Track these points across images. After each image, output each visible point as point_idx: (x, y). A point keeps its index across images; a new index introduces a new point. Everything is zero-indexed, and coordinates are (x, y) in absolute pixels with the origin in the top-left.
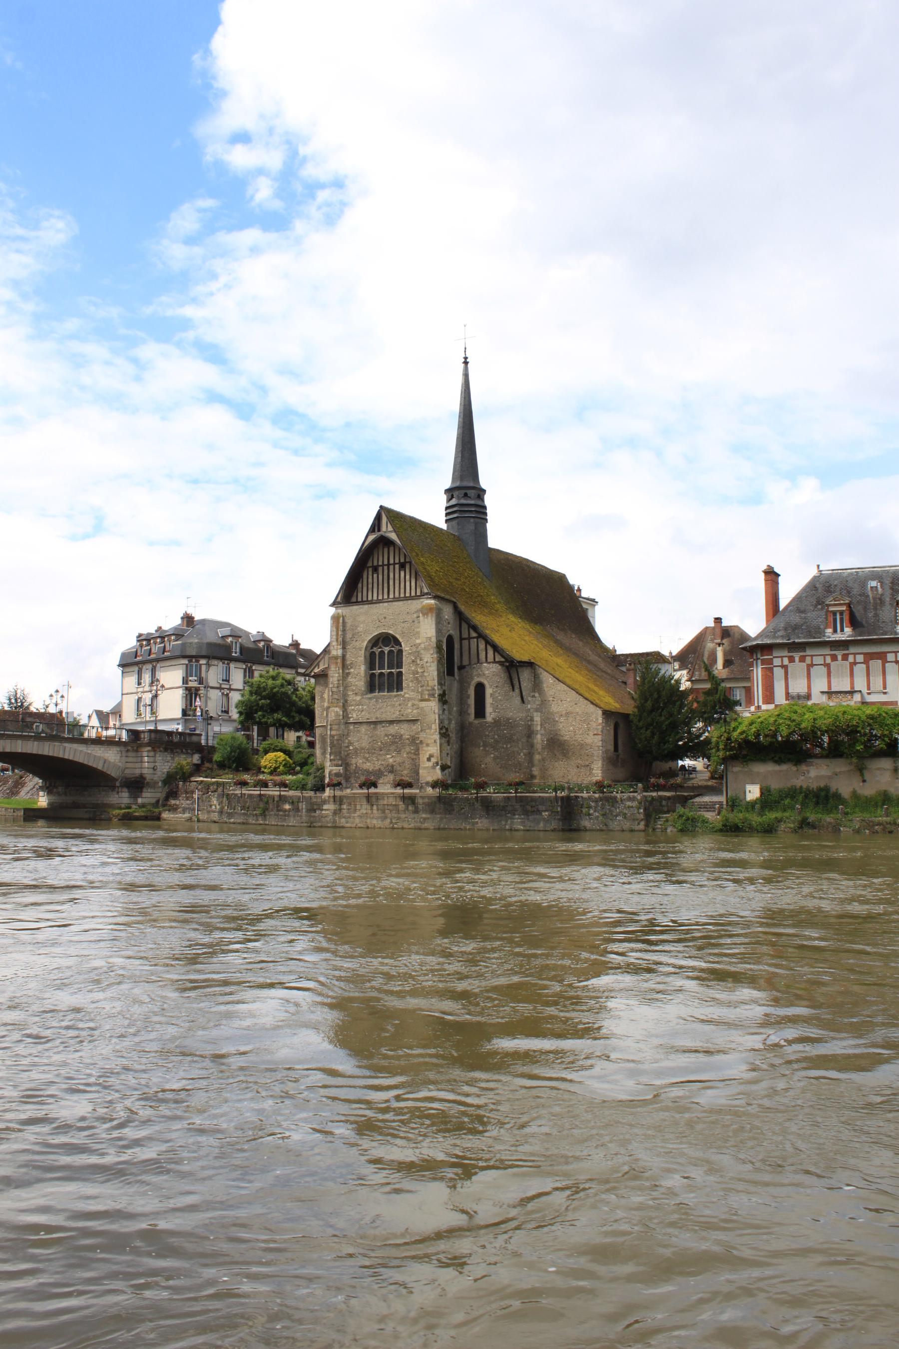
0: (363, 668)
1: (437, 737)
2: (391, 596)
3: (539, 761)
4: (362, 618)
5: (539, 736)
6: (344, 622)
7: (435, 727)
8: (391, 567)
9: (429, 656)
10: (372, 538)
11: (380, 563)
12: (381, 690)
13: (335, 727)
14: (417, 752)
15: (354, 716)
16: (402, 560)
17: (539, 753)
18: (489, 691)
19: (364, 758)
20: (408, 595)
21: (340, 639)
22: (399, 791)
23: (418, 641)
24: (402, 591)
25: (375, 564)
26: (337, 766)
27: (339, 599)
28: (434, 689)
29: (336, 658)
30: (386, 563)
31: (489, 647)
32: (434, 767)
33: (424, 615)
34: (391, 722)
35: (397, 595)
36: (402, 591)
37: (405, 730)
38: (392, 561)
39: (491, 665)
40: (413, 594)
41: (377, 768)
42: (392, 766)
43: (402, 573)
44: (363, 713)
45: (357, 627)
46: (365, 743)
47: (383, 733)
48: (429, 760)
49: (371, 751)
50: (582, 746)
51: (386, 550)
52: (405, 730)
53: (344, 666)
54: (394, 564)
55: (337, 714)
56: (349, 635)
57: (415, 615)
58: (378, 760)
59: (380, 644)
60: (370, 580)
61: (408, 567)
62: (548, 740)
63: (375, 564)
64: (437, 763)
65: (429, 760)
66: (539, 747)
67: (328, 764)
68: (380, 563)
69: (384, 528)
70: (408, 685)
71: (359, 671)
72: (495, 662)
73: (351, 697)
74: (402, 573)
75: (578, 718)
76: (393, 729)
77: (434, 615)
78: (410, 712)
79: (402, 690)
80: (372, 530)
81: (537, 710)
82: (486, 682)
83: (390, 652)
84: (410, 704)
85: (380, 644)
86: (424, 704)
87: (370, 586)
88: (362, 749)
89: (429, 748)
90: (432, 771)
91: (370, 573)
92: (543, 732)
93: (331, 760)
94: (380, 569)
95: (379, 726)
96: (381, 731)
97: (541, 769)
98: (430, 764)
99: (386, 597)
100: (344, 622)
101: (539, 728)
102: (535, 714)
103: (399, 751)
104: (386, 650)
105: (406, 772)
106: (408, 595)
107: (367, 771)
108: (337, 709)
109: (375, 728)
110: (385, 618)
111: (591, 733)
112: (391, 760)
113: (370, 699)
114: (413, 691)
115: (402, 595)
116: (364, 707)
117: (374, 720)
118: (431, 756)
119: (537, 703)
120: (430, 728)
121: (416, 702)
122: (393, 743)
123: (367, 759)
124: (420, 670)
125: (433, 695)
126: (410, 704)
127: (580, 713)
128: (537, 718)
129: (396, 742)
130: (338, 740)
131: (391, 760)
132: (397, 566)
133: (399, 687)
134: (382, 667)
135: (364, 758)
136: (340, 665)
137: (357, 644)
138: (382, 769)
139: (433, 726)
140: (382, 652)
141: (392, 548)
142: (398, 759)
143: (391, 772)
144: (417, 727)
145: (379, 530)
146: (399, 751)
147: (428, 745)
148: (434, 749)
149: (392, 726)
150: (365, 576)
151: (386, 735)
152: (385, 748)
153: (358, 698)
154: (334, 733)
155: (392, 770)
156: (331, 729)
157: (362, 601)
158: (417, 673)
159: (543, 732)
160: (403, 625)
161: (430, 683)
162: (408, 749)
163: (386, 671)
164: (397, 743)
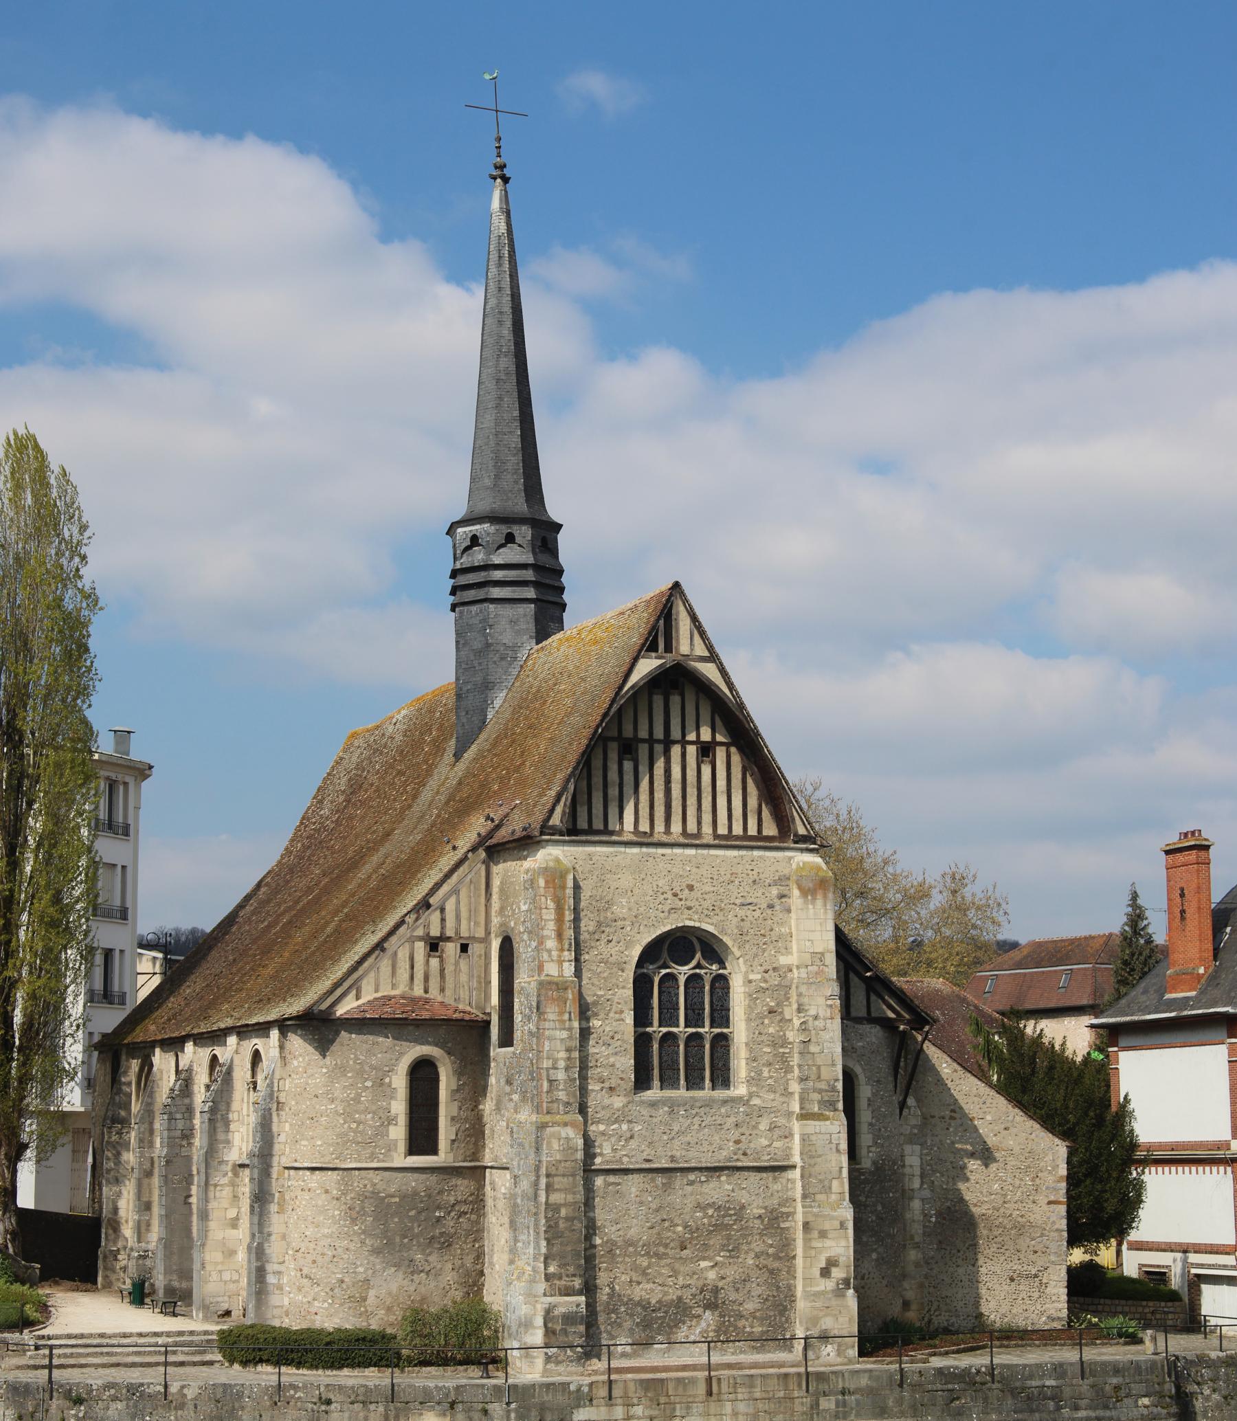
0: (629, 1018)
1: (848, 1213)
2: (676, 827)
3: (917, 1265)
4: (626, 880)
5: (916, 1204)
6: (577, 887)
7: (841, 1186)
8: (676, 751)
9: (821, 1001)
10: (647, 666)
11: (643, 734)
12: (668, 1080)
13: (559, 1182)
14: (785, 1253)
15: (605, 1154)
16: (706, 735)
17: (917, 1246)
18: (865, 1092)
19: (635, 1268)
20: (723, 830)
21: (569, 933)
22: (884, 1366)
23: (784, 960)
24: (707, 817)
25: (628, 732)
26: (568, 1292)
27: (556, 820)
28: (834, 1089)
29: (561, 986)
30: (659, 733)
31: (854, 979)
32: (839, 1293)
33: (804, 892)
34: (715, 1170)
35: (692, 827)
36: (707, 817)
37: (751, 1194)
38: (676, 734)
39: (866, 1028)
40: (738, 830)
41: (673, 1295)
42: (716, 1290)
43: (706, 770)
44: (633, 1144)
45: (609, 903)
46: (637, 1228)
47: (690, 1202)
48: (825, 1272)
49: (655, 1250)
50: (1021, 1229)
51: (658, 701)
52: (751, 1194)
53: (584, 1011)
54: (684, 743)
55: (569, 1148)
56: (587, 925)
57: (775, 891)
58: (675, 1274)
59: (665, 955)
60: (613, 775)
61: (720, 753)
62: (939, 1214)
63: (628, 732)
64: (846, 1282)
65: (825, 1272)
66: (917, 1229)
67: (542, 1286)
68: (643, 734)
69: (684, 648)
70: (760, 1073)
71: (617, 1025)
72: (871, 1020)
73: (597, 1097)
74: (706, 770)
75: (1012, 1162)
76: (718, 1190)
77: (830, 895)
78: (762, 1145)
79: (726, 1083)
80: (650, 646)
81: (911, 1140)
82: (858, 1070)
83: (693, 979)
84: (764, 1125)
85: (665, 955)
86: (813, 1126)
87: (613, 792)
88: (630, 1243)
89: (828, 1243)
90: (834, 1302)
91: (613, 756)
92: (927, 1193)
93: (548, 1277)
94: (643, 750)
95: (679, 1180)
96: (687, 1197)
97: (921, 1286)
98: (829, 1285)
99: (660, 827)
100: (577, 887)
101: (916, 1184)
102: (908, 1149)
103: (734, 1252)
104: (683, 972)
105: (750, 1306)
106: (723, 830)
107: (644, 1305)
108: (569, 1132)
109: (667, 1187)
110: (691, 888)
111: (1042, 1200)
112: (712, 1275)
113: (653, 1104)
114: (772, 1090)
115: (707, 829)
116: (640, 1126)
117: (665, 1164)
118: (831, 1263)
119: (913, 1121)
120: (828, 1190)
121: (782, 1121)
122: (718, 1227)
123: (644, 1273)
124: (791, 1036)
125: (831, 1105)
126: (764, 1125)
127: (1017, 1150)
128: (913, 1160)
129: (726, 1226)
130: (567, 1219)
131: (712, 1275)
132: (692, 750)
133: (722, 1077)
134: (668, 1017)
135: (635, 1268)
136: (572, 1007)
137: (613, 949)
138: (687, 1295)
139: (835, 1184)
140: (672, 977)
141: (675, 700)
142: (732, 1272)
143: (711, 1306)
144: (776, 1185)
145: (668, 648)
146: (734, 1252)
147: (823, 1234)
148: (842, 1246)
149: (713, 1184)
150: (597, 763)
151: (699, 1206)
152: (693, 1241)
153: (618, 1102)
154: (556, 1198)
155: (712, 1300)
156: (549, 1188)
157: (590, 831)
158: (785, 1042)
159: (927, 1193)
160: (741, 913)
161: (825, 1073)
162: (757, 1246)
163: (681, 1030)
164: (727, 1227)
